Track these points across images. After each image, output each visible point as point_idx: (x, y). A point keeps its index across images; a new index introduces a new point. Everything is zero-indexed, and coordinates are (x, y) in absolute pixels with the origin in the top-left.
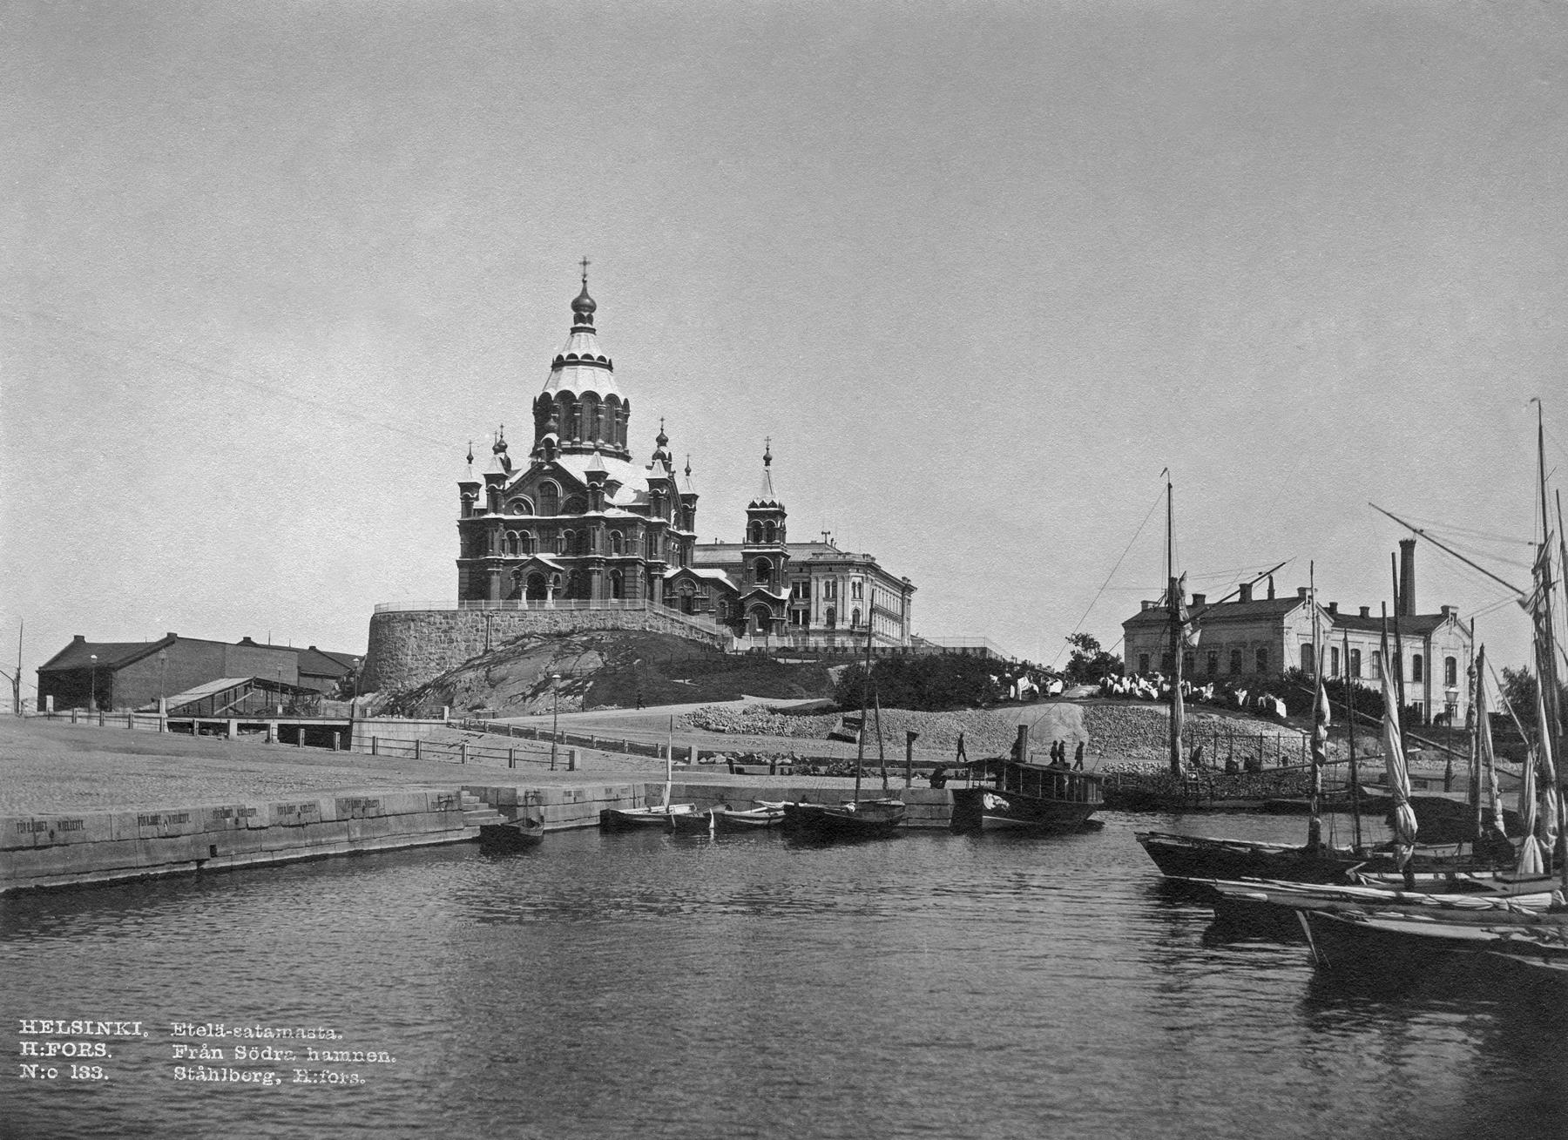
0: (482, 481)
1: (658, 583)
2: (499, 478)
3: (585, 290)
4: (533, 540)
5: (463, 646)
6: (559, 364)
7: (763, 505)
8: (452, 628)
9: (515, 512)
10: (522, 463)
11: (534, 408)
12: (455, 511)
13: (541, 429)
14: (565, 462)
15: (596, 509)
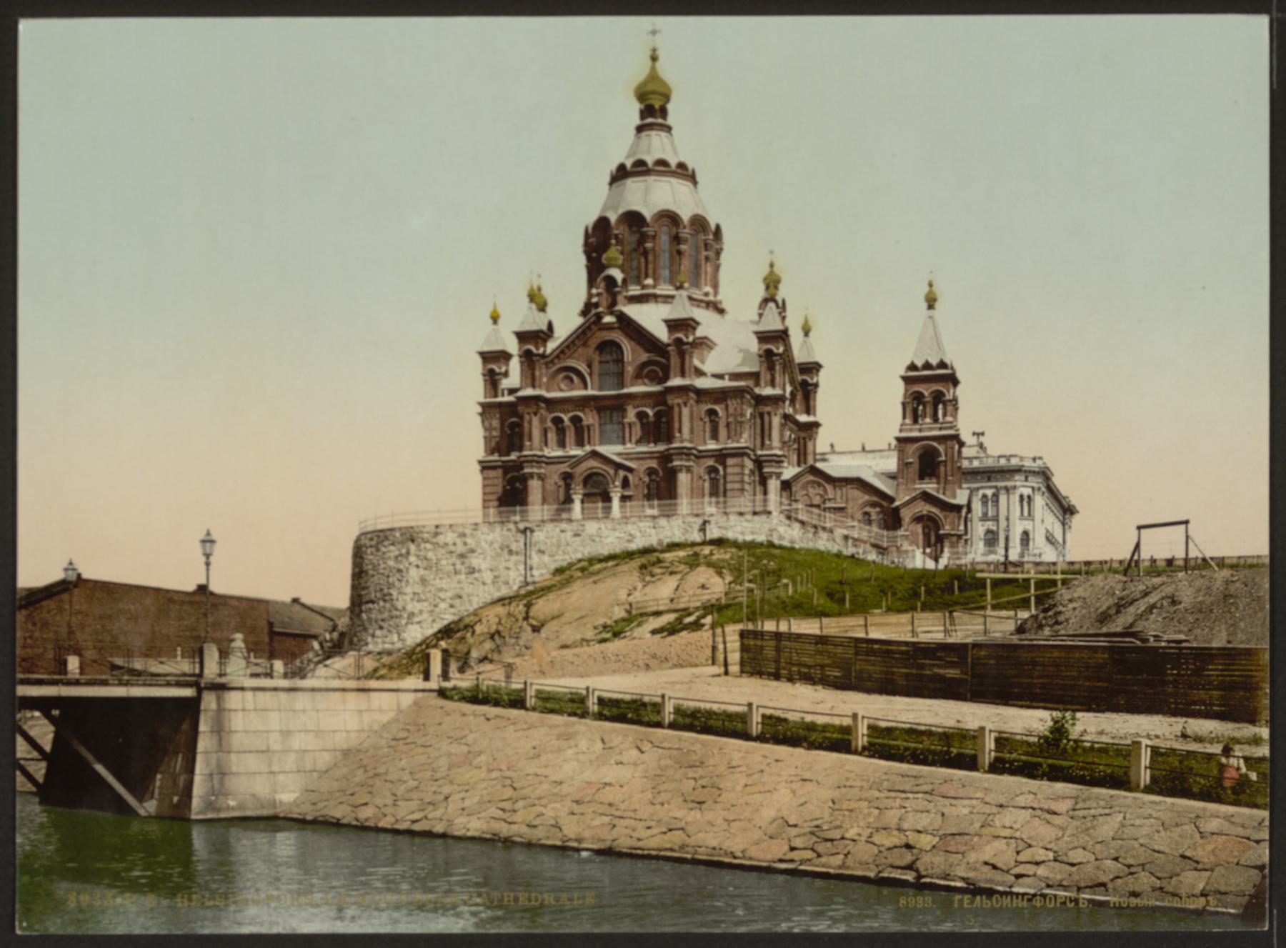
0: (513, 346)
1: (773, 485)
2: (541, 336)
3: (653, 69)
4: (589, 427)
5: (488, 577)
6: (621, 174)
7: (927, 366)
8: (473, 551)
9: (563, 386)
10: (566, 321)
11: (586, 244)
12: (475, 390)
13: (595, 268)
14: (636, 312)
15: (683, 375)
